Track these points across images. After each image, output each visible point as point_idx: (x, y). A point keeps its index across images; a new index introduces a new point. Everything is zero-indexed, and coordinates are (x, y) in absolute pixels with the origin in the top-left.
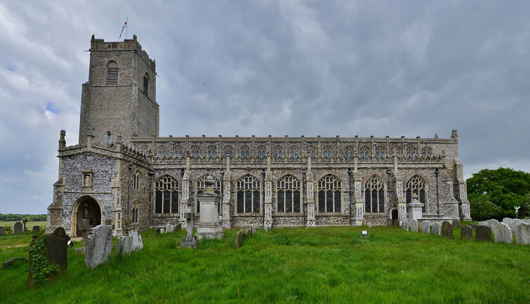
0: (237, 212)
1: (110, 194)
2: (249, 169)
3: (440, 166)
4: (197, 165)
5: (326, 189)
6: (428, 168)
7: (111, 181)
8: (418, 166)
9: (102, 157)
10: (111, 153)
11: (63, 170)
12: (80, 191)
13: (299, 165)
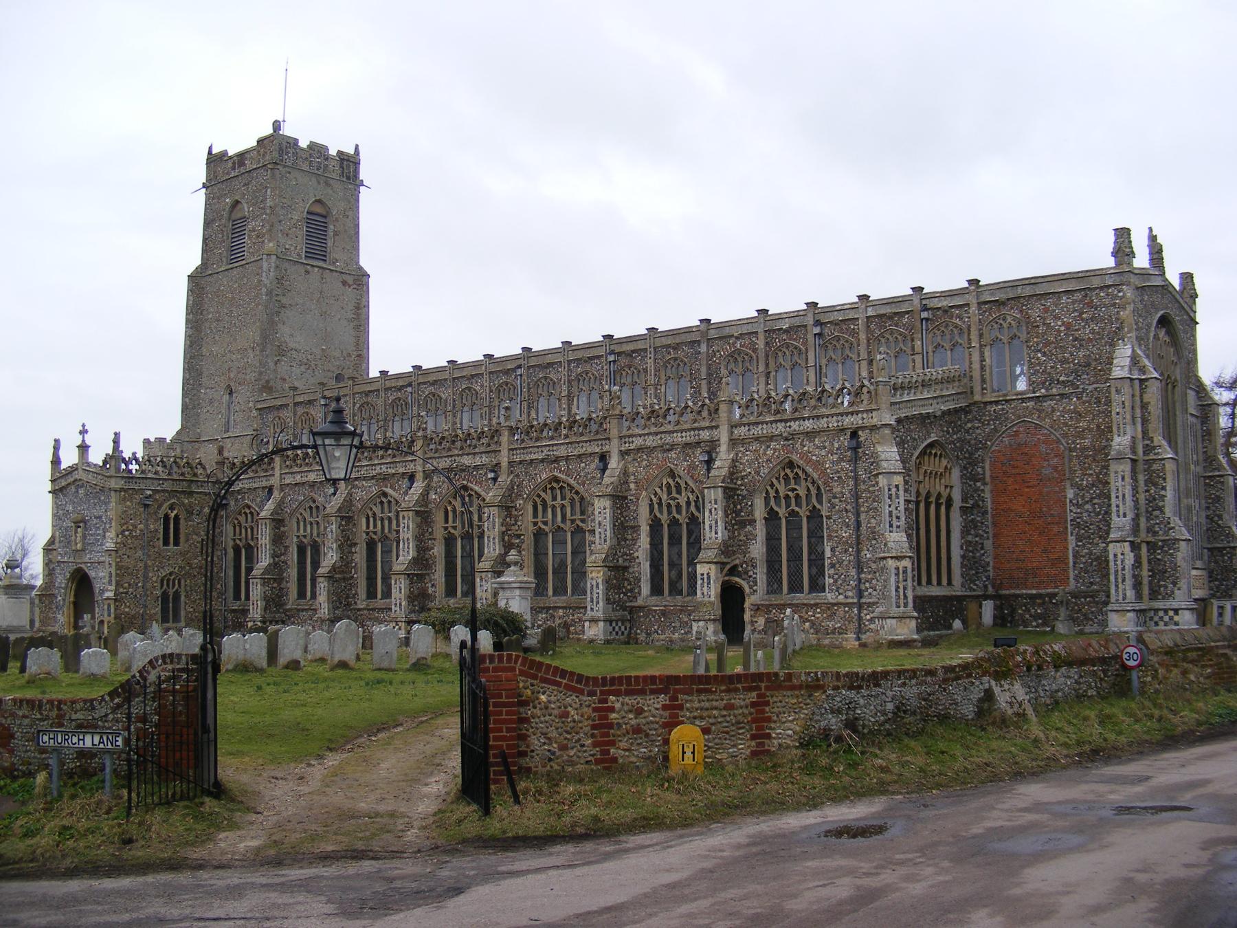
0: (364, 596)
2: (384, 478)
6: (826, 431)
8: (795, 425)
13: (483, 455)
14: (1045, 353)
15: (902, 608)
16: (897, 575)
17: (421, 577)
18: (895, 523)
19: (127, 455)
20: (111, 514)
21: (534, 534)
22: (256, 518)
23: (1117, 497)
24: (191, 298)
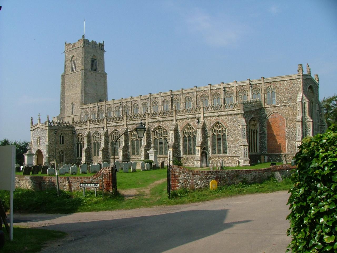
2: (116, 126)
3: (236, 112)
6: (227, 115)
8: (219, 113)
14: (280, 95)
15: (246, 157)
16: (245, 149)
17: (126, 151)
18: (244, 137)
19: (51, 121)
20: (47, 136)
21: (154, 140)
22: (83, 136)
23: (298, 131)
24: (62, 80)
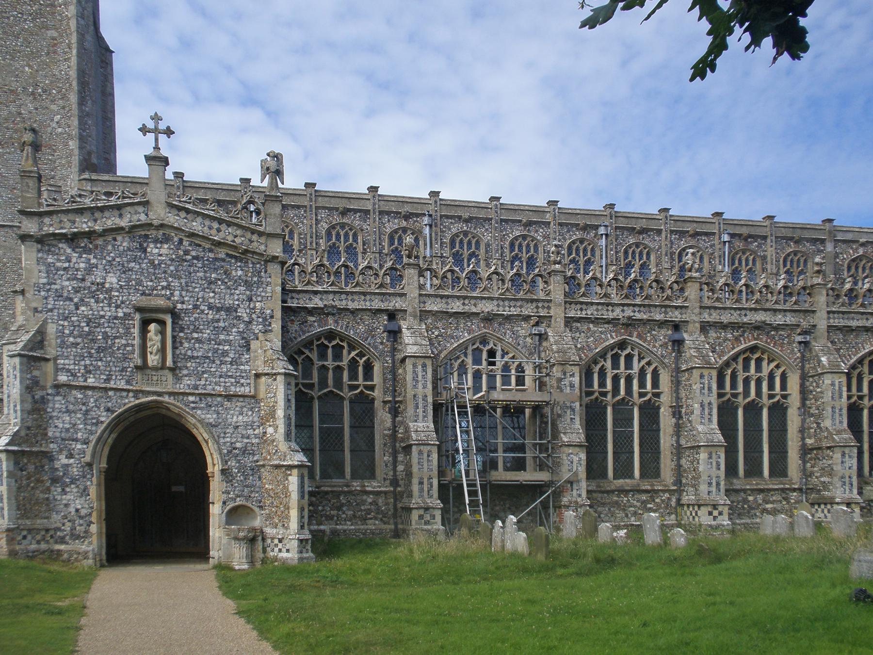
1: (247, 400)
4: (444, 301)
5: (609, 396)
7: (248, 350)
9: (211, 251)
10: (248, 235)
11: (43, 293)
12: (122, 384)
13: (788, 314)
